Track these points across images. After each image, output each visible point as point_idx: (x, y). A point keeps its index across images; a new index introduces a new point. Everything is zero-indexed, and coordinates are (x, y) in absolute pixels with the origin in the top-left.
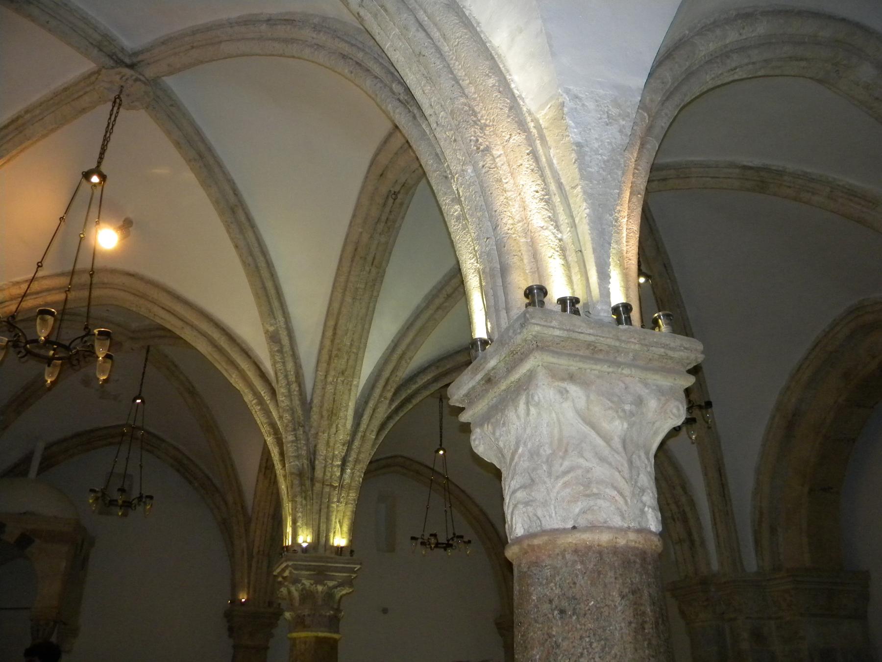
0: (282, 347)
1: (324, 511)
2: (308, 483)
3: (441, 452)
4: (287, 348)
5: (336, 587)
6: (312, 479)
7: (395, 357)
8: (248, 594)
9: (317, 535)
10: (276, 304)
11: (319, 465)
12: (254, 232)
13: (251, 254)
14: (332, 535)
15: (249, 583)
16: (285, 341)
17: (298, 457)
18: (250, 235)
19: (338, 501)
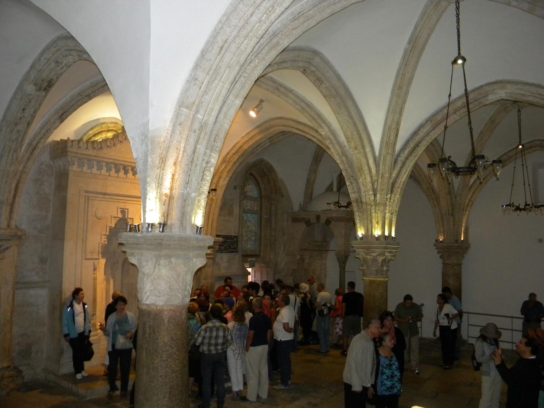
0: (331, 140)
1: (369, 218)
2: (360, 204)
3: (520, 147)
4: (334, 141)
5: (377, 256)
6: (362, 202)
7: (387, 130)
8: (444, 236)
9: (367, 230)
10: (319, 121)
11: (363, 194)
12: (293, 94)
13: (297, 104)
14: (374, 230)
15: (444, 231)
16: (332, 137)
17: (354, 192)
18: (291, 95)
19: (375, 212)
